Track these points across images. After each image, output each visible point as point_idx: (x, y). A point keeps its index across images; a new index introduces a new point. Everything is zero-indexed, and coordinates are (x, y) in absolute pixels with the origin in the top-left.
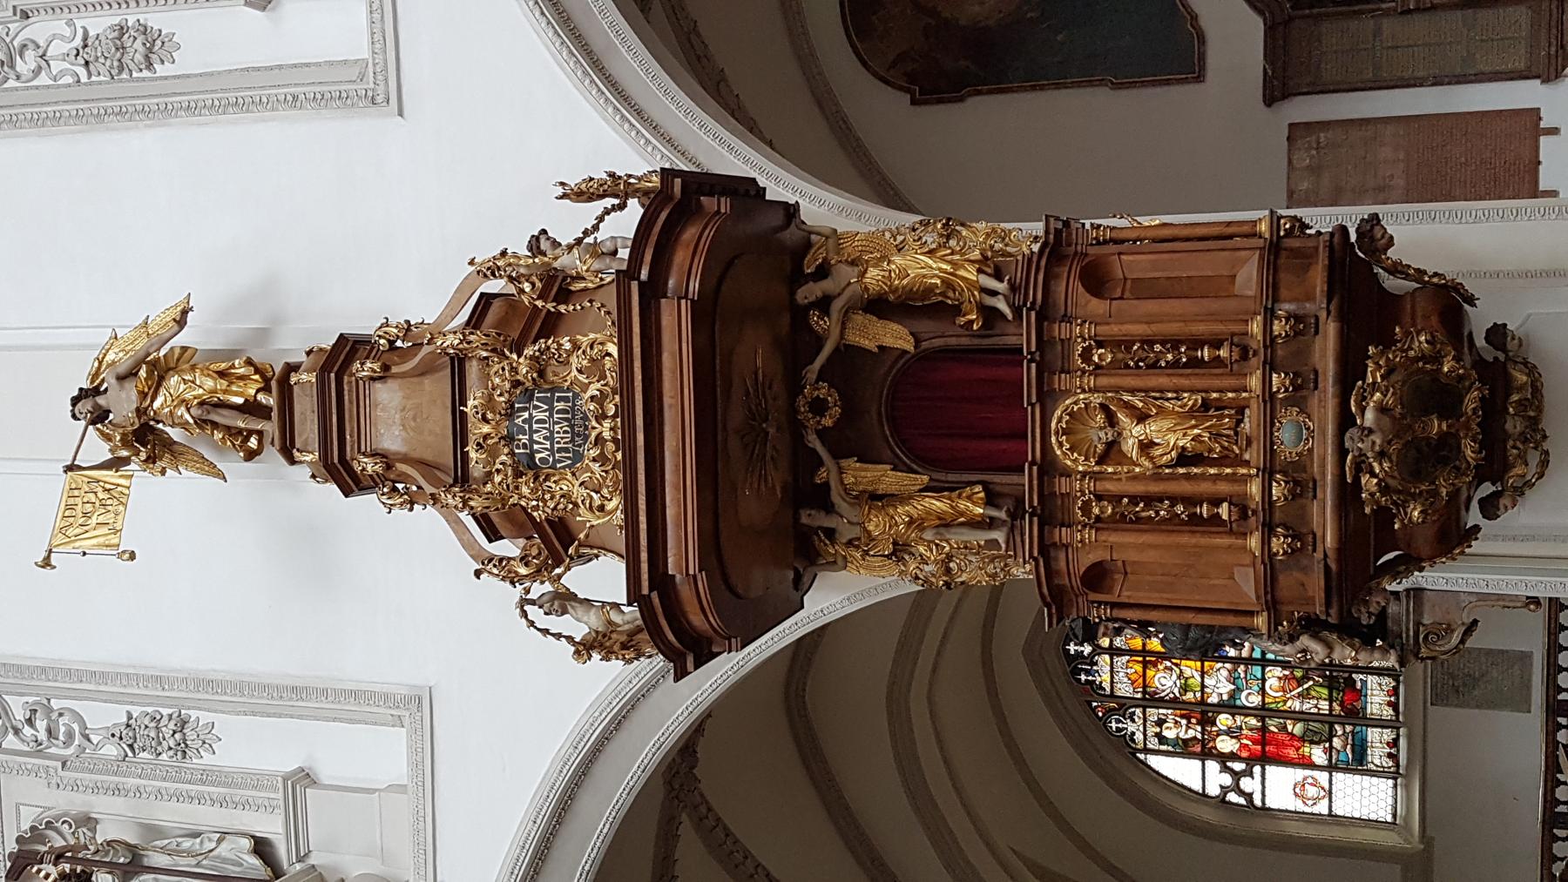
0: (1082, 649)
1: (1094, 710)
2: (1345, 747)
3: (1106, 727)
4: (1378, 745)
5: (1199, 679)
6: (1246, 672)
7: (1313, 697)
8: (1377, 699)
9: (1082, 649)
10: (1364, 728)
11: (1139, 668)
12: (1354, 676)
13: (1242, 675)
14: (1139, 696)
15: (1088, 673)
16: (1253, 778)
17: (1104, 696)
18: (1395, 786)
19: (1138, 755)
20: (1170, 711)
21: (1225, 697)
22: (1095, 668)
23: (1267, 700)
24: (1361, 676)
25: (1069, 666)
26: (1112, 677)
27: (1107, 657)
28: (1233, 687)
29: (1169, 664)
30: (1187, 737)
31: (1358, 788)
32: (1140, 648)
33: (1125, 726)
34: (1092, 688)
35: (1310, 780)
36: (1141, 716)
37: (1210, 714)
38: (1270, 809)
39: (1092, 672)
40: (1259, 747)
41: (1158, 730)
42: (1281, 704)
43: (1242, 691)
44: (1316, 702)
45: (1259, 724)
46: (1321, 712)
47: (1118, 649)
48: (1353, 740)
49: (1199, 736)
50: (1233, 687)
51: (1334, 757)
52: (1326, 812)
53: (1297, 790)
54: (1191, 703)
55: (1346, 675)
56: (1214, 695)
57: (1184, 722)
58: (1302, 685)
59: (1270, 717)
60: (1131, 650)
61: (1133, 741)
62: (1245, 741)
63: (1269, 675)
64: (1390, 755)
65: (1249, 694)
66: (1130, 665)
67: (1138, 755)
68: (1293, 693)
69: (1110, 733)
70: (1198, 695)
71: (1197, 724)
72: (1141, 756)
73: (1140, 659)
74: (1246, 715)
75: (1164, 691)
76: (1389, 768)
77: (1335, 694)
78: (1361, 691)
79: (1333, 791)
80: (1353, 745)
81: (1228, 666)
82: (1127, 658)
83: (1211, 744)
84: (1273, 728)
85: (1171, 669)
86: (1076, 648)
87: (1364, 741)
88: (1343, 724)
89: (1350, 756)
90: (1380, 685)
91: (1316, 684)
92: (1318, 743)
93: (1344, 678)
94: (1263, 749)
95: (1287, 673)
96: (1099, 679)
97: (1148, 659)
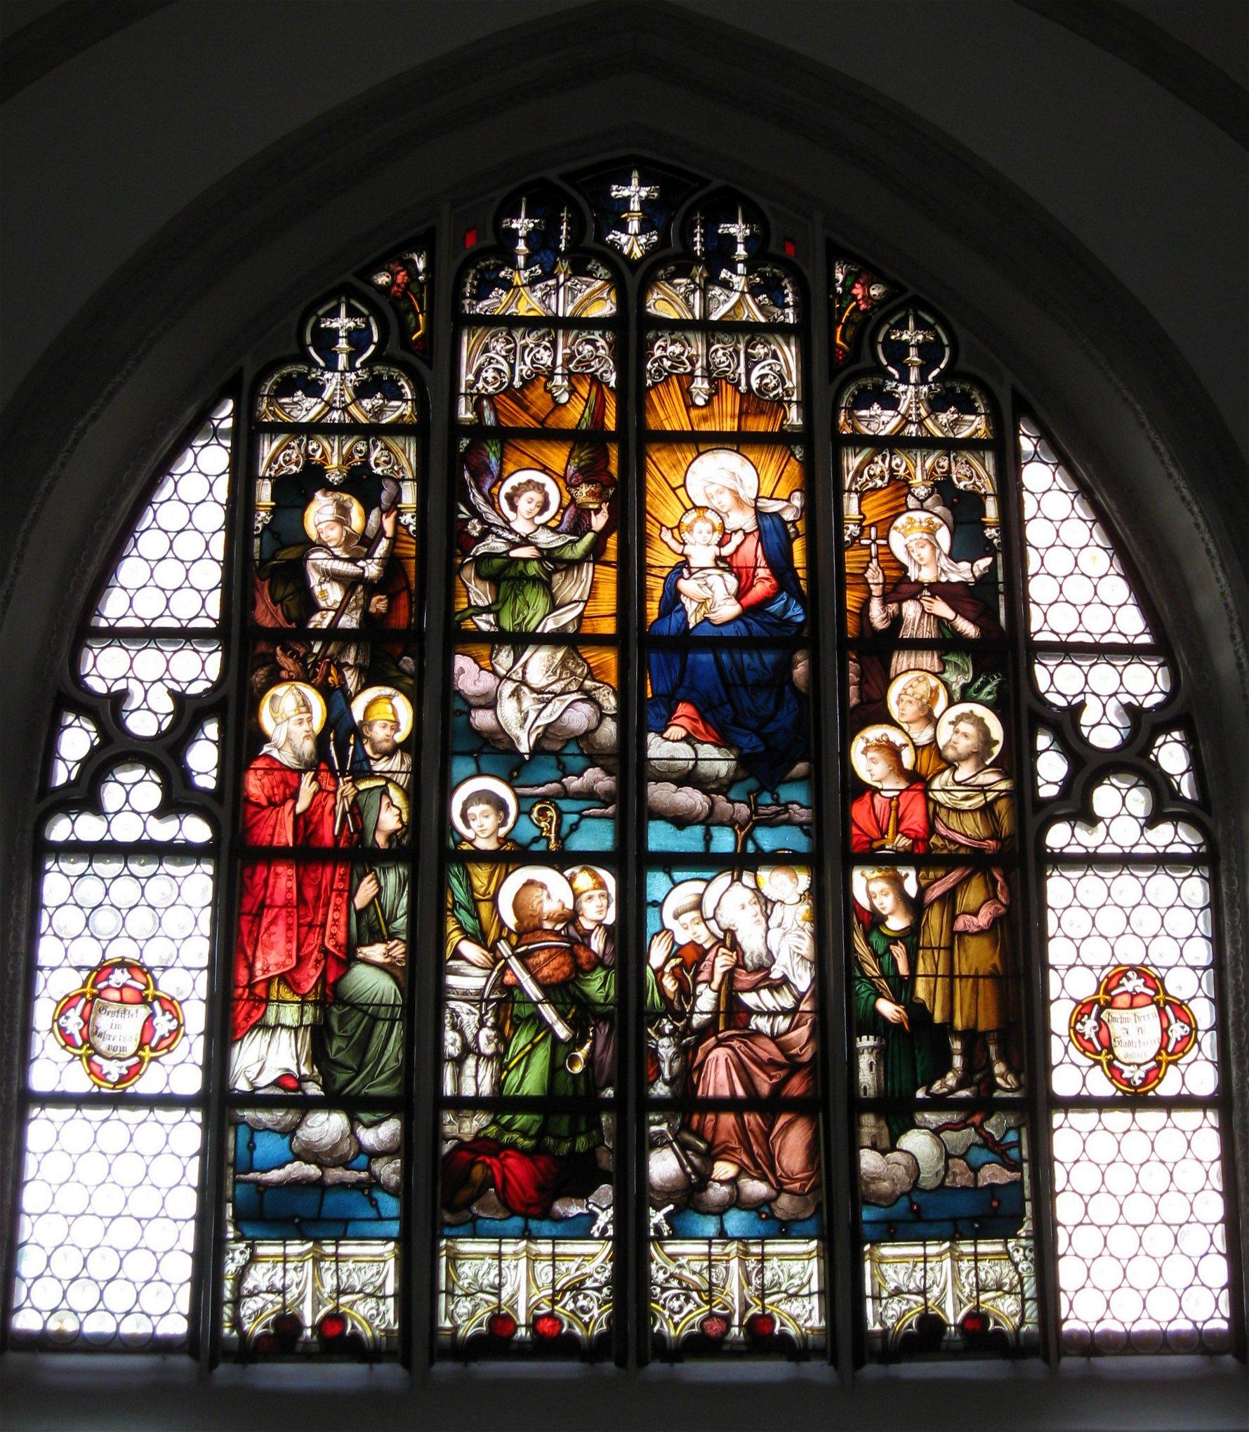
0: (634, 226)
1: (395, 256)
2: (308, 1154)
3: (334, 294)
4: (330, 1282)
5: (550, 625)
6: (588, 795)
7: (503, 1040)
8: (515, 1276)
9: (634, 226)
10: (394, 1228)
11: (575, 414)
12: (605, 1191)
13: (574, 783)
14: (465, 413)
15: (541, 242)
16: (160, 813)
17: (458, 296)
18: (155, 1345)
19: (229, 406)
20: (408, 519)
21: (482, 719)
22: (563, 266)
23: (481, 876)
24: (604, 1218)
25: (563, 177)
26: (531, 323)
27: (604, 308)
28: (524, 748)
29: (599, 522)
30: (314, 579)
31: (145, 1203)
32: (652, 424)
33: (342, 361)
34: (482, 253)
35: (163, 1024)
36: (388, 418)
37: (408, 663)
38: (38, 875)
39: (547, 256)
40: (286, 836)
41: (334, 477)
42: (469, 922)
43: (510, 782)
44: (488, 1049)
45: (381, 840)
46: (448, 1071)
47: (644, 352)
48: (342, 1185)
49: (321, 621)
50: (524, 748)
51: (264, 1116)
52: (41, 1078)
53: (120, 977)
54: (450, 595)
55: (606, 1160)
56: (486, 682)
57: (372, 570)
58: (549, 998)
59: (413, 883)
60: (643, 392)
61: (287, 387)
62: (307, 788)
63: (584, 880)
64: (287, 1323)
65: (501, 806)
66: (584, 390)
67: (229, 406)
68: (514, 963)
69: (310, 310)
70: (484, 623)
71: (367, 617)
72: (224, 416)
73: (610, 423)
74: (414, 794)
75: (492, 501)
76: (237, 1323)
77: (522, 1120)
78: (546, 1214)
79: (124, 1114)
80: (318, 1185)
81: (609, 729)
82: (612, 379)
83: (287, 663)
84: (366, 891)
85: (579, 526)
86: (635, 206)
87: (342, 1229)
88: (404, 1148)
89: (275, 1175)
90: (577, 1288)
91: (560, 1052)
92: (318, 1055)
93: (591, 1153)
94: (277, 854)
95: (597, 944)
96: (520, 278)
97: (614, 452)
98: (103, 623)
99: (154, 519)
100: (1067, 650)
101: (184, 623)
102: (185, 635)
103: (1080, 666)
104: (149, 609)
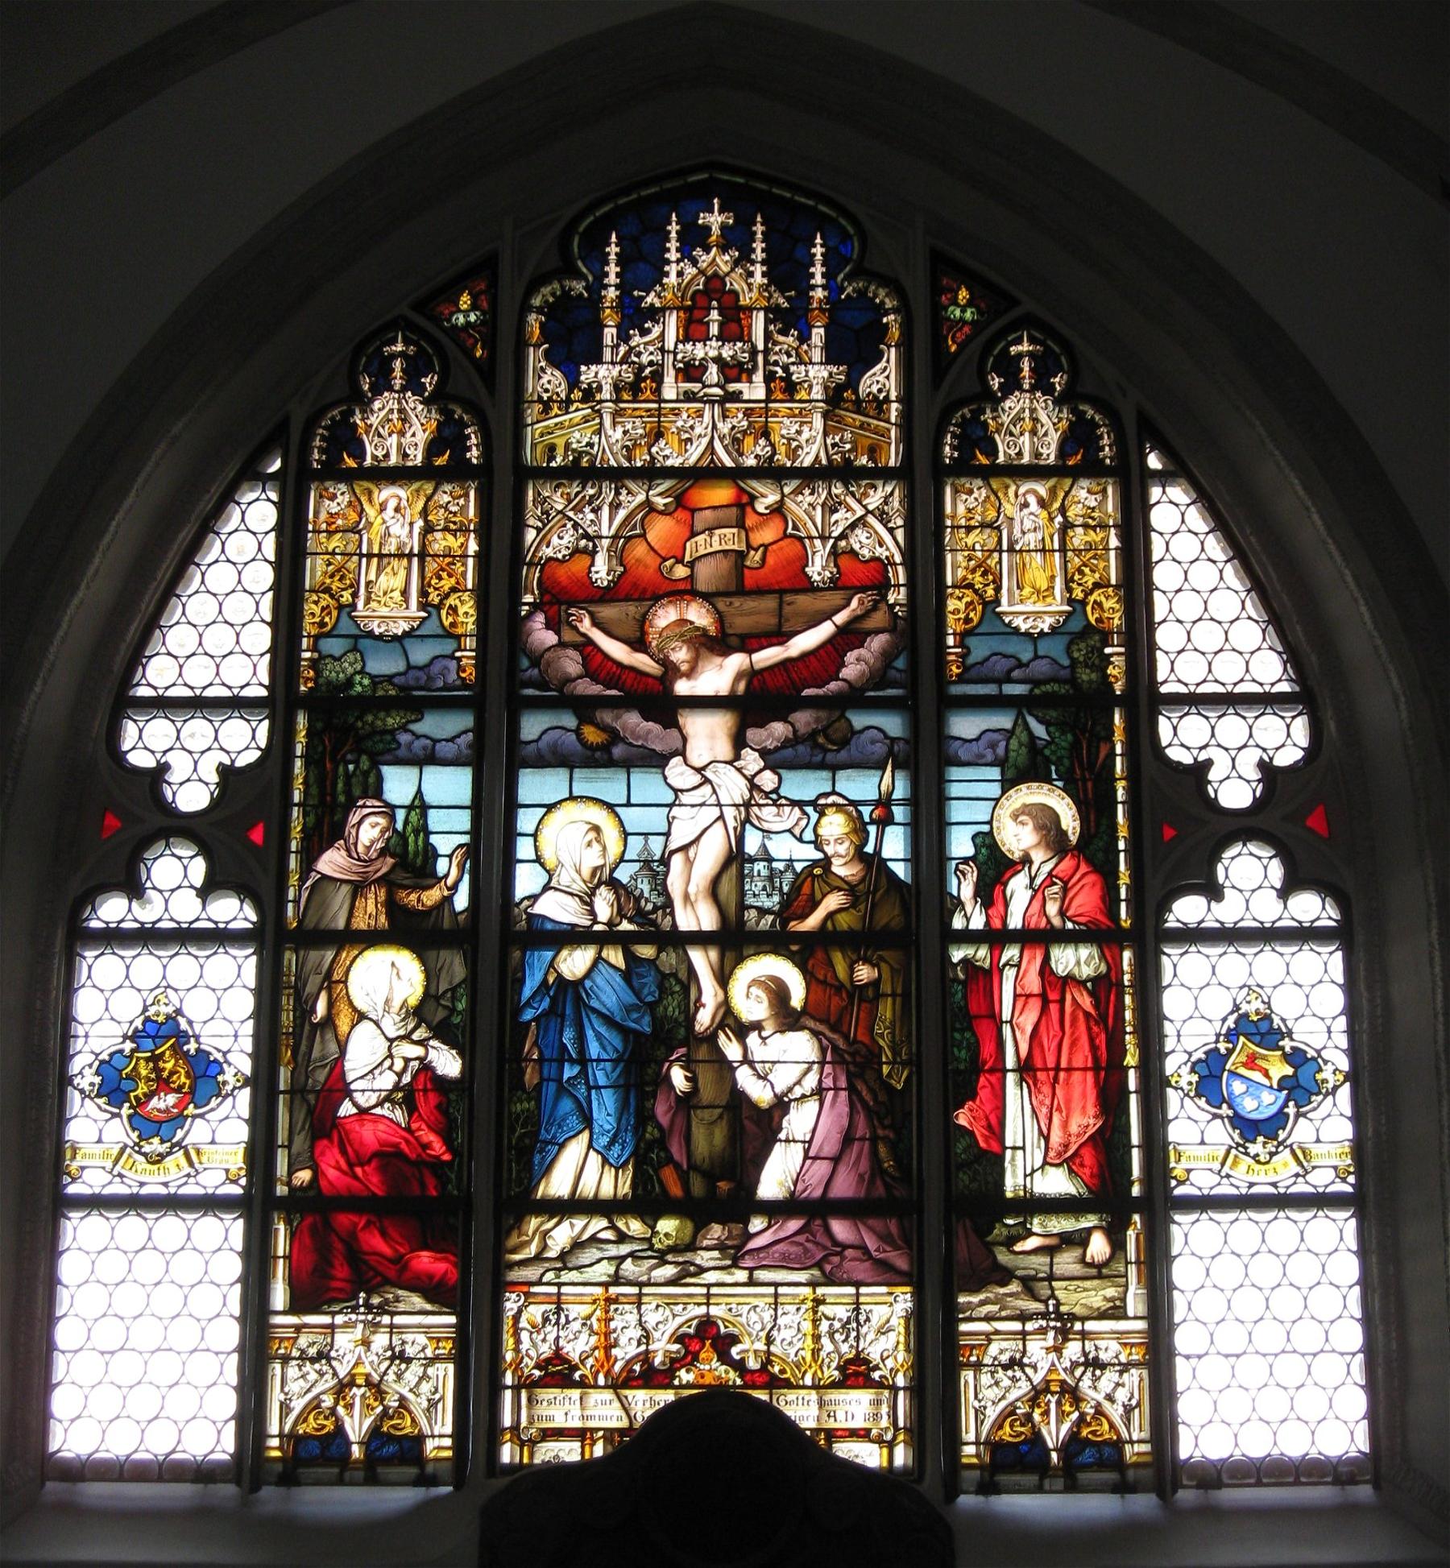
98: (143, 692)
99: (203, 582)
100: (1193, 701)
101: (236, 691)
102: (235, 705)
103: (1207, 718)
104: (199, 677)
